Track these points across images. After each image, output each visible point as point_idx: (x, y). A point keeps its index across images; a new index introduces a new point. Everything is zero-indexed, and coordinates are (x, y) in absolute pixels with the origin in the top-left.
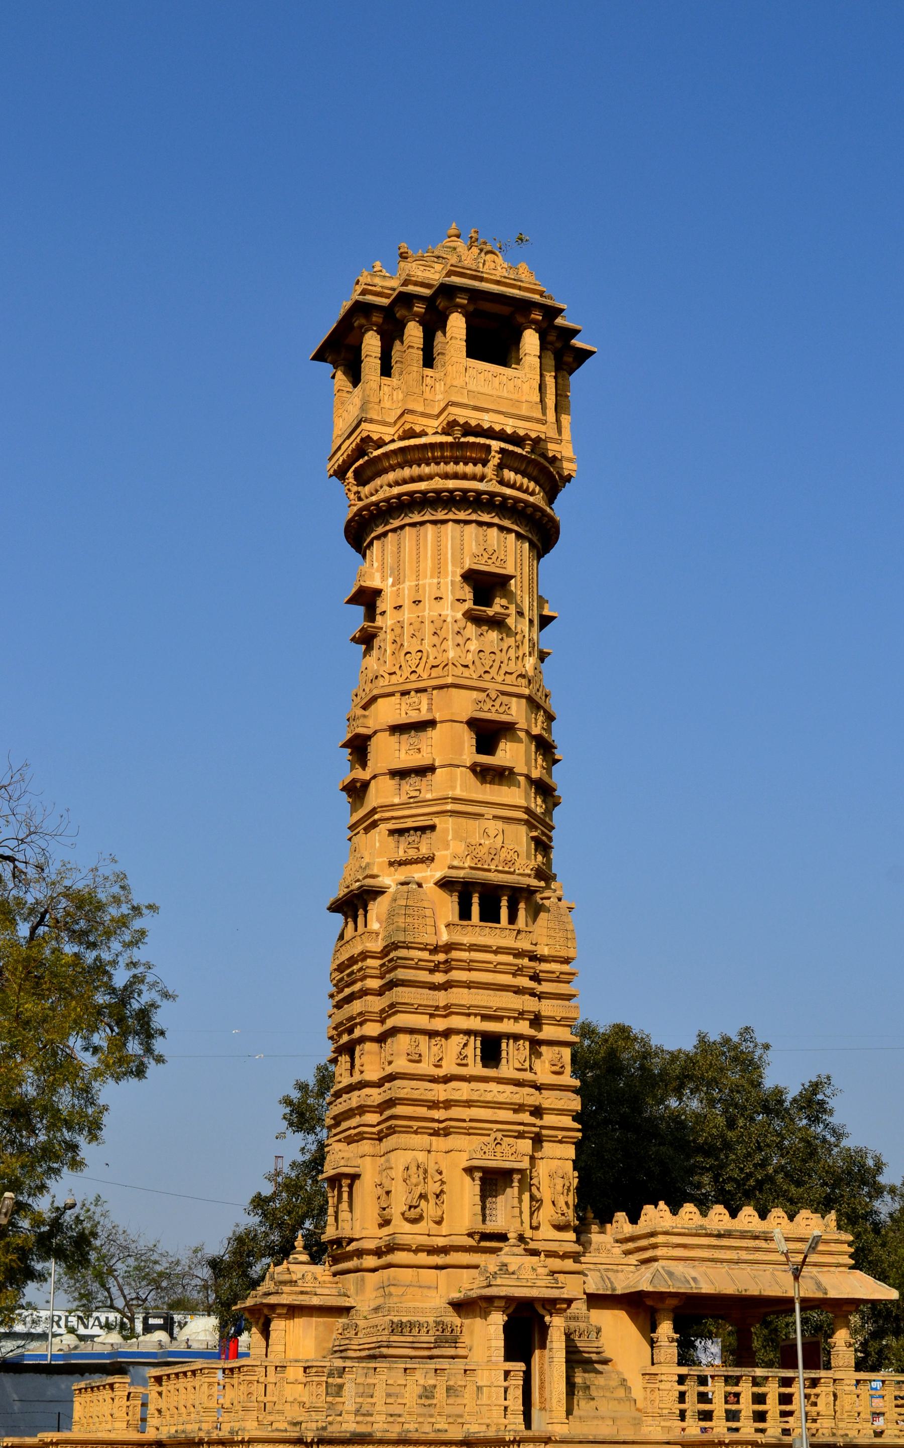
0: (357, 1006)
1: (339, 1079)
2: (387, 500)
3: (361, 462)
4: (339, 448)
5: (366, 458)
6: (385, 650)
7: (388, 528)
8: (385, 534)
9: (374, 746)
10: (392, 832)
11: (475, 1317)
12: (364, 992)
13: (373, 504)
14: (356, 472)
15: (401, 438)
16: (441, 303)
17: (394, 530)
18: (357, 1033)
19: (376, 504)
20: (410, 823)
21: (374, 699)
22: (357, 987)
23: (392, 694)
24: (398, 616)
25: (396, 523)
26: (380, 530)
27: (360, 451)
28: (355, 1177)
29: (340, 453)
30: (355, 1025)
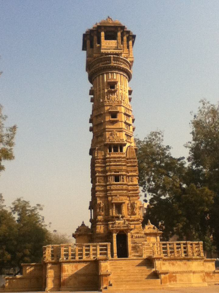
0: (124, 168)
1: (111, 181)
2: (123, 68)
3: (117, 56)
4: (110, 49)
5: (118, 56)
6: (119, 97)
7: (119, 73)
8: (118, 73)
9: (119, 115)
10: (126, 134)
11: (151, 236)
12: (124, 165)
13: (120, 67)
14: (113, 57)
15: (124, 57)
16: (131, 37)
17: (120, 74)
18: (120, 173)
19: (121, 67)
20: (130, 135)
21: (121, 106)
22: (123, 164)
23: (124, 107)
24: (122, 91)
25: (121, 73)
26: (117, 72)
27: (116, 54)
28: (124, 203)
29: (109, 50)
30: (120, 172)
